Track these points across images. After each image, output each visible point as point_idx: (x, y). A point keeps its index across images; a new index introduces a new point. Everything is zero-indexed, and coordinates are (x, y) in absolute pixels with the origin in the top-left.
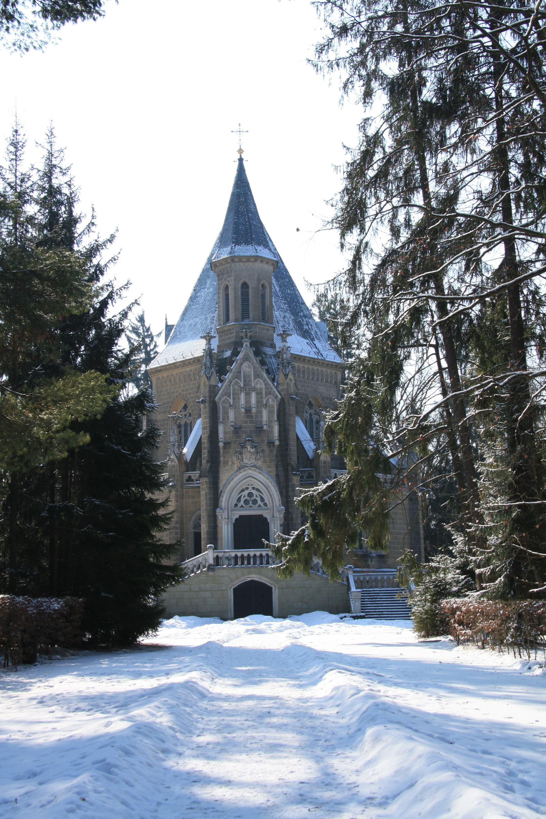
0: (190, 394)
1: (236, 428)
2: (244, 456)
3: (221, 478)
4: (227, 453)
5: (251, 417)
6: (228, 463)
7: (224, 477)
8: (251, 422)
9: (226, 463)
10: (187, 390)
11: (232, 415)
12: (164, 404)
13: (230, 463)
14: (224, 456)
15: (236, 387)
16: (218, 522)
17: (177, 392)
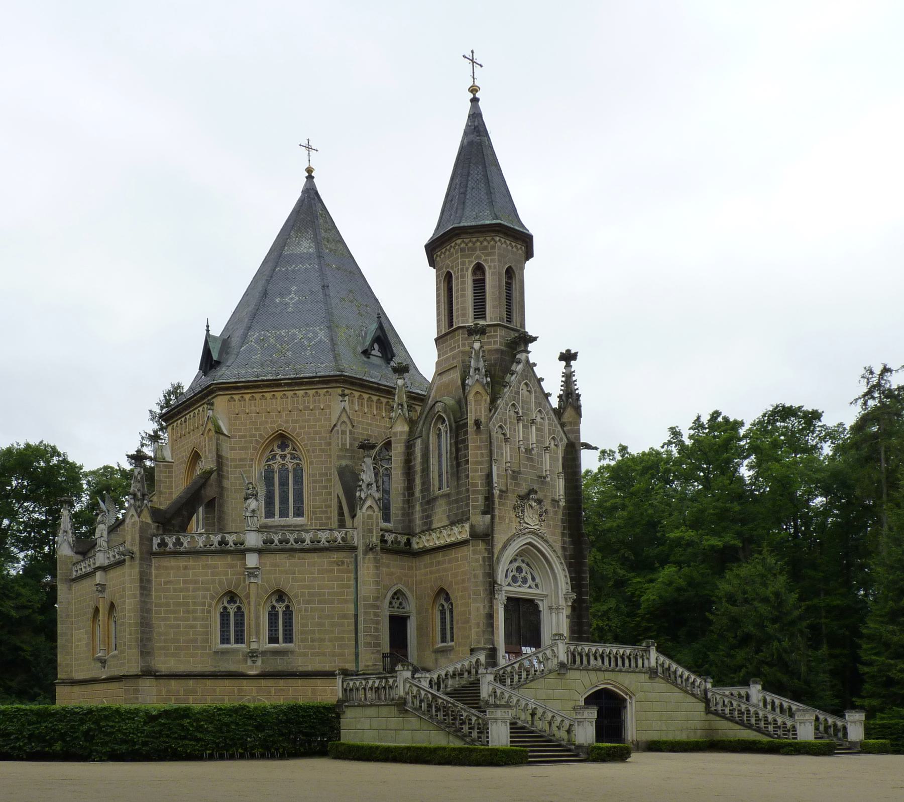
0: (301, 428)
1: (514, 472)
2: (526, 514)
3: (495, 540)
4: (504, 504)
5: (531, 460)
6: (505, 520)
7: (500, 539)
8: (533, 467)
9: (502, 518)
10: (297, 421)
11: (507, 451)
12: (244, 436)
13: (507, 521)
14: (499, 509)
15: (512, 413)
16: (495, 601)
17: (273, 422)
